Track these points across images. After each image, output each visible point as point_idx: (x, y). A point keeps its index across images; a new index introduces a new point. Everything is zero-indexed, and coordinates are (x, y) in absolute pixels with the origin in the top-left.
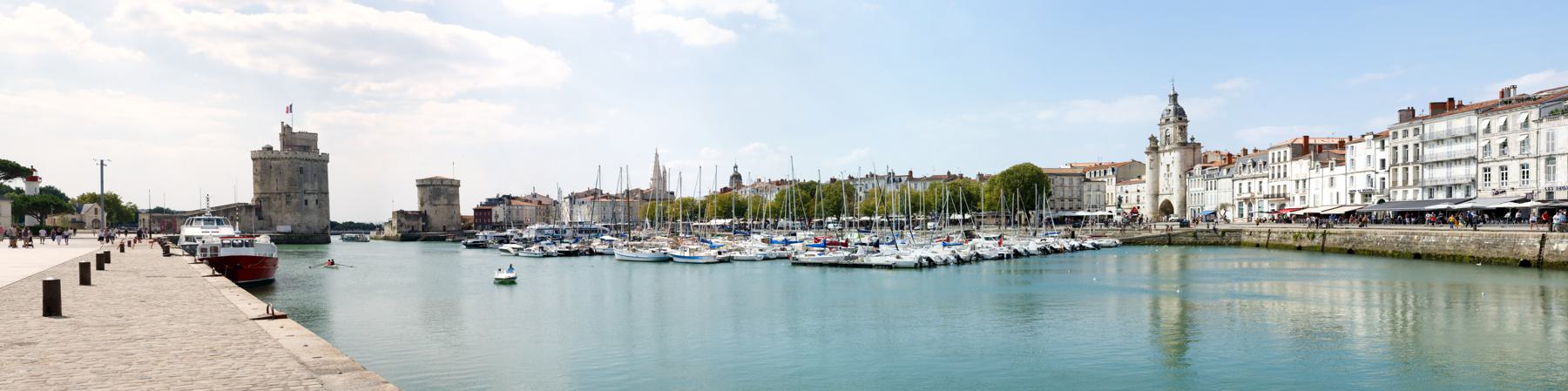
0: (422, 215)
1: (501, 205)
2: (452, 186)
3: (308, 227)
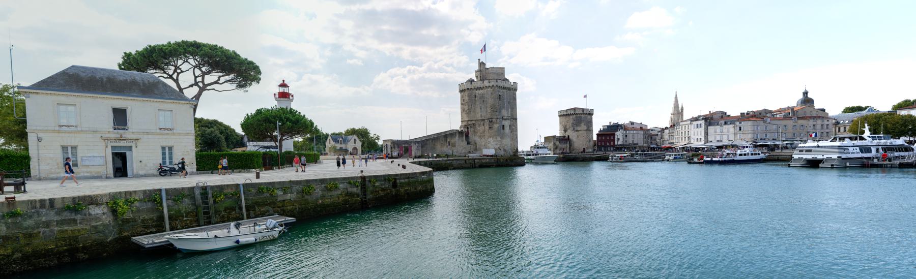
0: (564, 140)
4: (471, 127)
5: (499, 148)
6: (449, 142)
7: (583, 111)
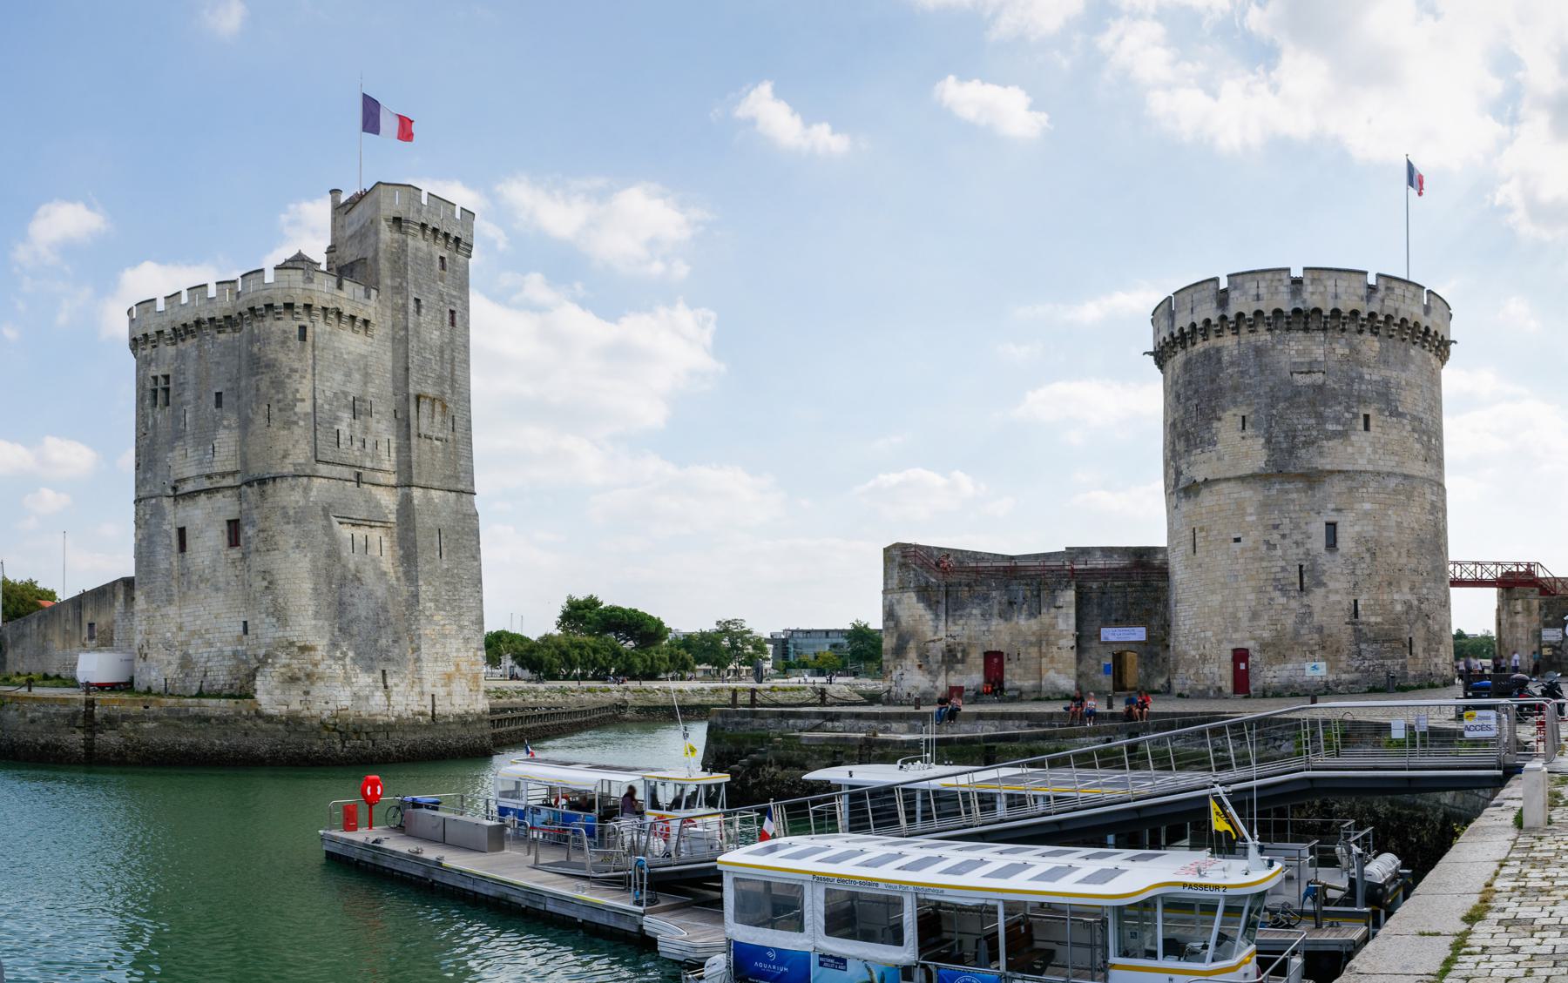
2: (1303, 319)
3: (186, 663)
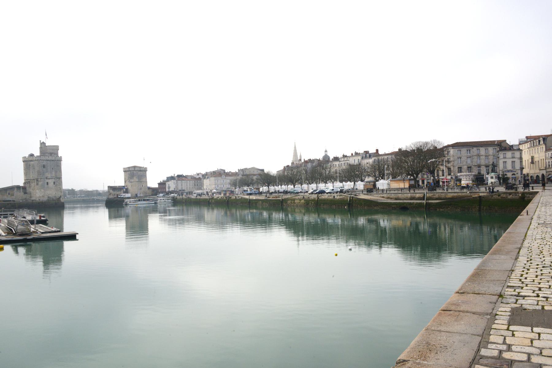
1: (172, 181)
2: (140, 171)
4: (28, 183)
5: (43, 196)
6: (9, 193)
7: (135, 169)
